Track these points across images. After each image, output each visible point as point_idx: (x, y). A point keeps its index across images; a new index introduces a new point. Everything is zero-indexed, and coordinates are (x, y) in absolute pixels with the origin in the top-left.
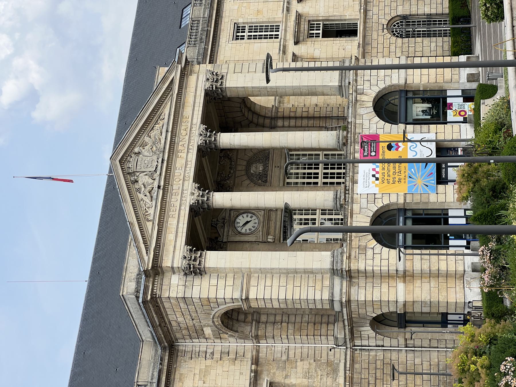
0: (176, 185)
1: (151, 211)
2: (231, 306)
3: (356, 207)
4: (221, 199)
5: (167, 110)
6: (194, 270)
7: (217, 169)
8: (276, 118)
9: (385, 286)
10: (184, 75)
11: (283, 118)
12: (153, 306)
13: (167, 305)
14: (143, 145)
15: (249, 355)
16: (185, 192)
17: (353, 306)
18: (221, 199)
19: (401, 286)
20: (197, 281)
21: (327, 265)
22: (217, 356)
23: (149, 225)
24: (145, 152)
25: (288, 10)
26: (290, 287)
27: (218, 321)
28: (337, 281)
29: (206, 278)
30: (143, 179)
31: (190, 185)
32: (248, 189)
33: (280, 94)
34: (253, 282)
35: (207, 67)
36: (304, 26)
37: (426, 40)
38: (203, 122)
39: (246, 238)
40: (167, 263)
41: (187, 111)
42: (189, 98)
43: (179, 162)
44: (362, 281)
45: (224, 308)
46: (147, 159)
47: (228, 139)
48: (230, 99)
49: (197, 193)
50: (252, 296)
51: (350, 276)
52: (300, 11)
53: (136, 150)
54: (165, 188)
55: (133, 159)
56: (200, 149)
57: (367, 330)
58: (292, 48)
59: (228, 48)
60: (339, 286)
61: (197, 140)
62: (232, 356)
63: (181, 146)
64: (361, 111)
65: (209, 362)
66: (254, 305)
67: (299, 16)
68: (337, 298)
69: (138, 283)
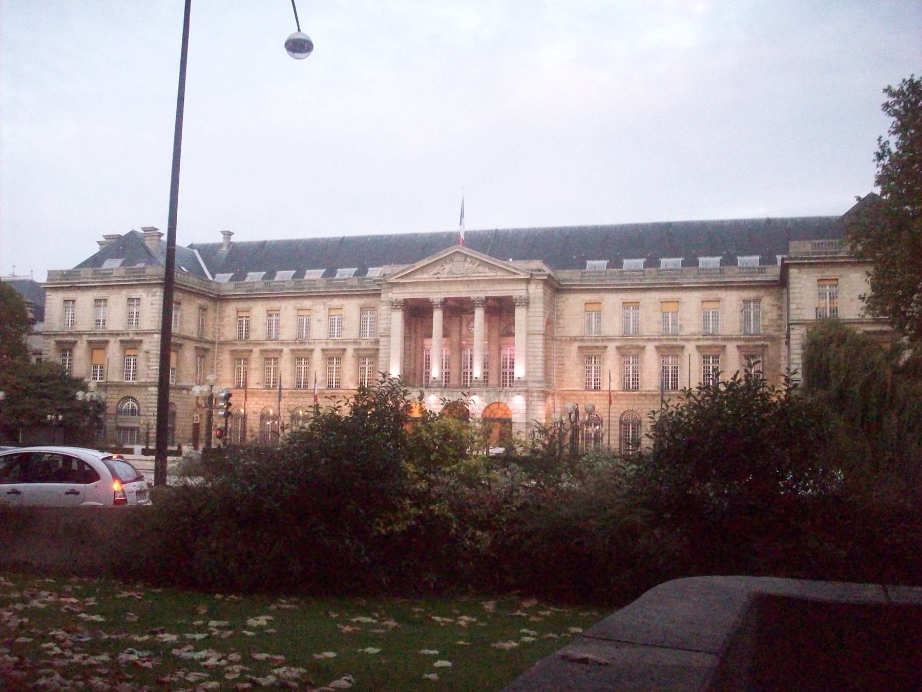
0: (445, 288)
1: (426, 276)
5: (500, 275)
6: (394, 305)
10: (528, 281)
16: (436, 295)
23: (417, 277)
24: (467, 265)
25: (649, 340)
39: (464, 328)
46: (459, 267)
49: (439, 300)
52: (647, 348)
53: (468, 260)
61: (473, 296)
64: (492, 394)
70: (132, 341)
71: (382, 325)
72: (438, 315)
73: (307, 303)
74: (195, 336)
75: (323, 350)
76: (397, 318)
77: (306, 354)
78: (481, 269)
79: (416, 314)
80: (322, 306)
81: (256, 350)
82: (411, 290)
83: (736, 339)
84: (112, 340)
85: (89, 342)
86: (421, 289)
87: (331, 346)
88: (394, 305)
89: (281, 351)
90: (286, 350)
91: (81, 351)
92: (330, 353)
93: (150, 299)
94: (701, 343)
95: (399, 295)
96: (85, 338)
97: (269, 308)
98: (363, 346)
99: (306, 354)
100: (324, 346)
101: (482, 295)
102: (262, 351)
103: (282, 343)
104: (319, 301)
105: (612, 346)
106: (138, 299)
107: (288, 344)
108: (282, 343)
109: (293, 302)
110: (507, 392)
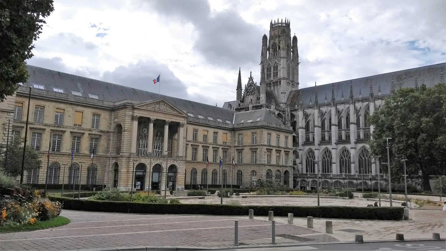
0: (156, 114)
1: (149, 108)
2: (123, 127)
3: (147, 159)
4: (151, 126)
5: (175, 112)
6: (133, 118)
7: (160, 125)
8: (172, 139)
9: (126, 166)
11: (172, 141)
12: (124, 107)
13: (124, 110)
14: (166, 106)
15: (109, 130)
16: (154, 117)
17: (121, 158)
18: (151, 126)
19: (125, 170)
20: (130, 119)
21: (132, 152)
22: (110, 122)
23: (146, 107)
26: (125, 166)
27: (119, 123)
28: (128, 154)
29: (131, 121)
30: (158, 106)
31: (155, 118)
32: (154, 132)
33: (178, 140)
34: (129, 133)
35: (186, 122)
36: (196, 147)
37: (190, 178)
38: (171, 122)
40: (135, 111)
41: (175, 118)
42: (178, 118)
43: (161, 115)
44: (127, 160)
45: (122, 125)
47: (167, 128)
48: (177, 128)
50: (125, 132)
51: (129, 157)
54: (155, 111)
55: (163, 104)
56: (165, 121)
57: (114, 161)
58: (190, 144)
59: (191, 128)
60: (127, 155)
61: (167, 120)
62: (109, 126)
63: (166, 116)
65: (108, 120)
66: (123, 133)
67: (198, 146)
68: (123, 154)
69: (130, 104)
71: (126, 126)
73: (62, 106)
75: (71, 132)
76: (136, 123)
77: (61, 133)
78: (169, 109)
80: (71, 109)
82: (142, 112)
83: (222, 146)
86: (146, 113)
87: (75, 131)
89: (45, 130)
92: (75, 135)
94: (213, 146)
95: (138, 114)
97: (37, 104)
98: (94, 132)
99: (61, 133)
100: (72, 130)
101: (170, 120)
104: (70, 106)
107: (50, 126)
108: (46, 125)
109: (53, 104)
110: (177, 160)
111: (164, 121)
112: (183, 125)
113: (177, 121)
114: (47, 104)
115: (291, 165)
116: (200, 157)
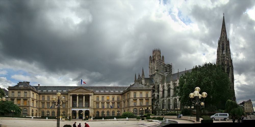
10: (91, 92)
16: (78, 94)
43: (81, 93)
54: (78, 92)
61: (83, 94)
70: (25, 99)
71: (69, 98)
72: (78, 97)
74: (36, 99)
76: (71, 97)
79: (74, 97)
81: (46, 102)
84: (22, 99)
85: (17, 99)
88: (70, 95)
90: (51, 102)
91: (15, 100)
93: (29, 92)
95: (71, 94)
96: (16, 98)
101: (85, 94)
102: (47, 102)
103: (50, 101)
105: (100, 102)
106: (27, 92)
108: (50, 101)
111: (82, 95)
112: (91, 95)
113: (88, 94)
114: (50, 95)
115: (150, 105)
116: (100, 107)
